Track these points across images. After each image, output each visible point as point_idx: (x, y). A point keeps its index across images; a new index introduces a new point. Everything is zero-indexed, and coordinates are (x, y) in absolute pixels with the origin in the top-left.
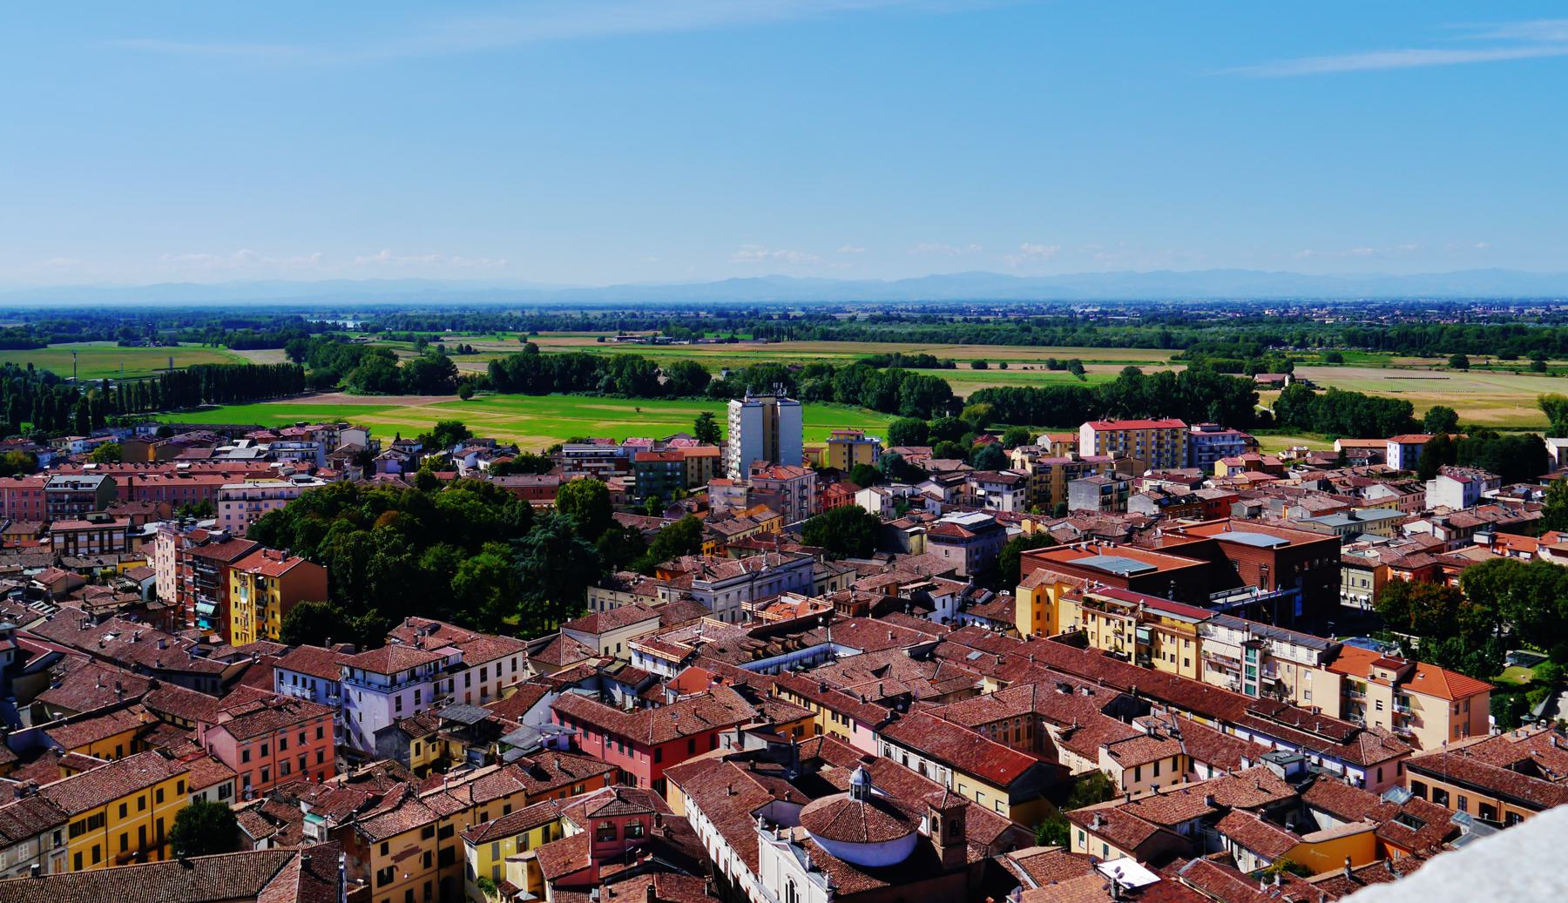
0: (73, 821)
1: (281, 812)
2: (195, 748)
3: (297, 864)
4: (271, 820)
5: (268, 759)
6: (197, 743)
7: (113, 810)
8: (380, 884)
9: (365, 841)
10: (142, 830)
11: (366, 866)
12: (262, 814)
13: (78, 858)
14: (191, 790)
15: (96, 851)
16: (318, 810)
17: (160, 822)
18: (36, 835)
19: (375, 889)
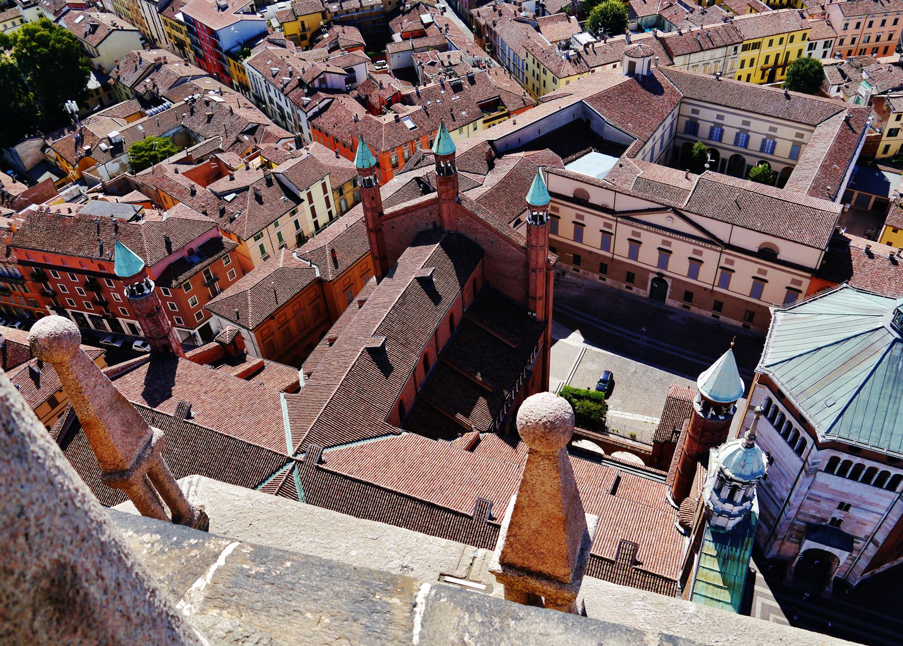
0: (745, 43)
1: (851, 73)
2: (821, 11)
3: (843, 115)
4: (844, 76)
5: (859, 31)
6: (823, 7)
7: (766, 42)
8: (888, 136)
9: (889, 110)
10: (778, 55)
11: (884, 123)
12: (840, 70)
13: (743, 62)
14: (809, 40)
15: (752, 60)
16: (871, 81)
17: (788, 53)
18: (726, 46)
19: (884, 137)
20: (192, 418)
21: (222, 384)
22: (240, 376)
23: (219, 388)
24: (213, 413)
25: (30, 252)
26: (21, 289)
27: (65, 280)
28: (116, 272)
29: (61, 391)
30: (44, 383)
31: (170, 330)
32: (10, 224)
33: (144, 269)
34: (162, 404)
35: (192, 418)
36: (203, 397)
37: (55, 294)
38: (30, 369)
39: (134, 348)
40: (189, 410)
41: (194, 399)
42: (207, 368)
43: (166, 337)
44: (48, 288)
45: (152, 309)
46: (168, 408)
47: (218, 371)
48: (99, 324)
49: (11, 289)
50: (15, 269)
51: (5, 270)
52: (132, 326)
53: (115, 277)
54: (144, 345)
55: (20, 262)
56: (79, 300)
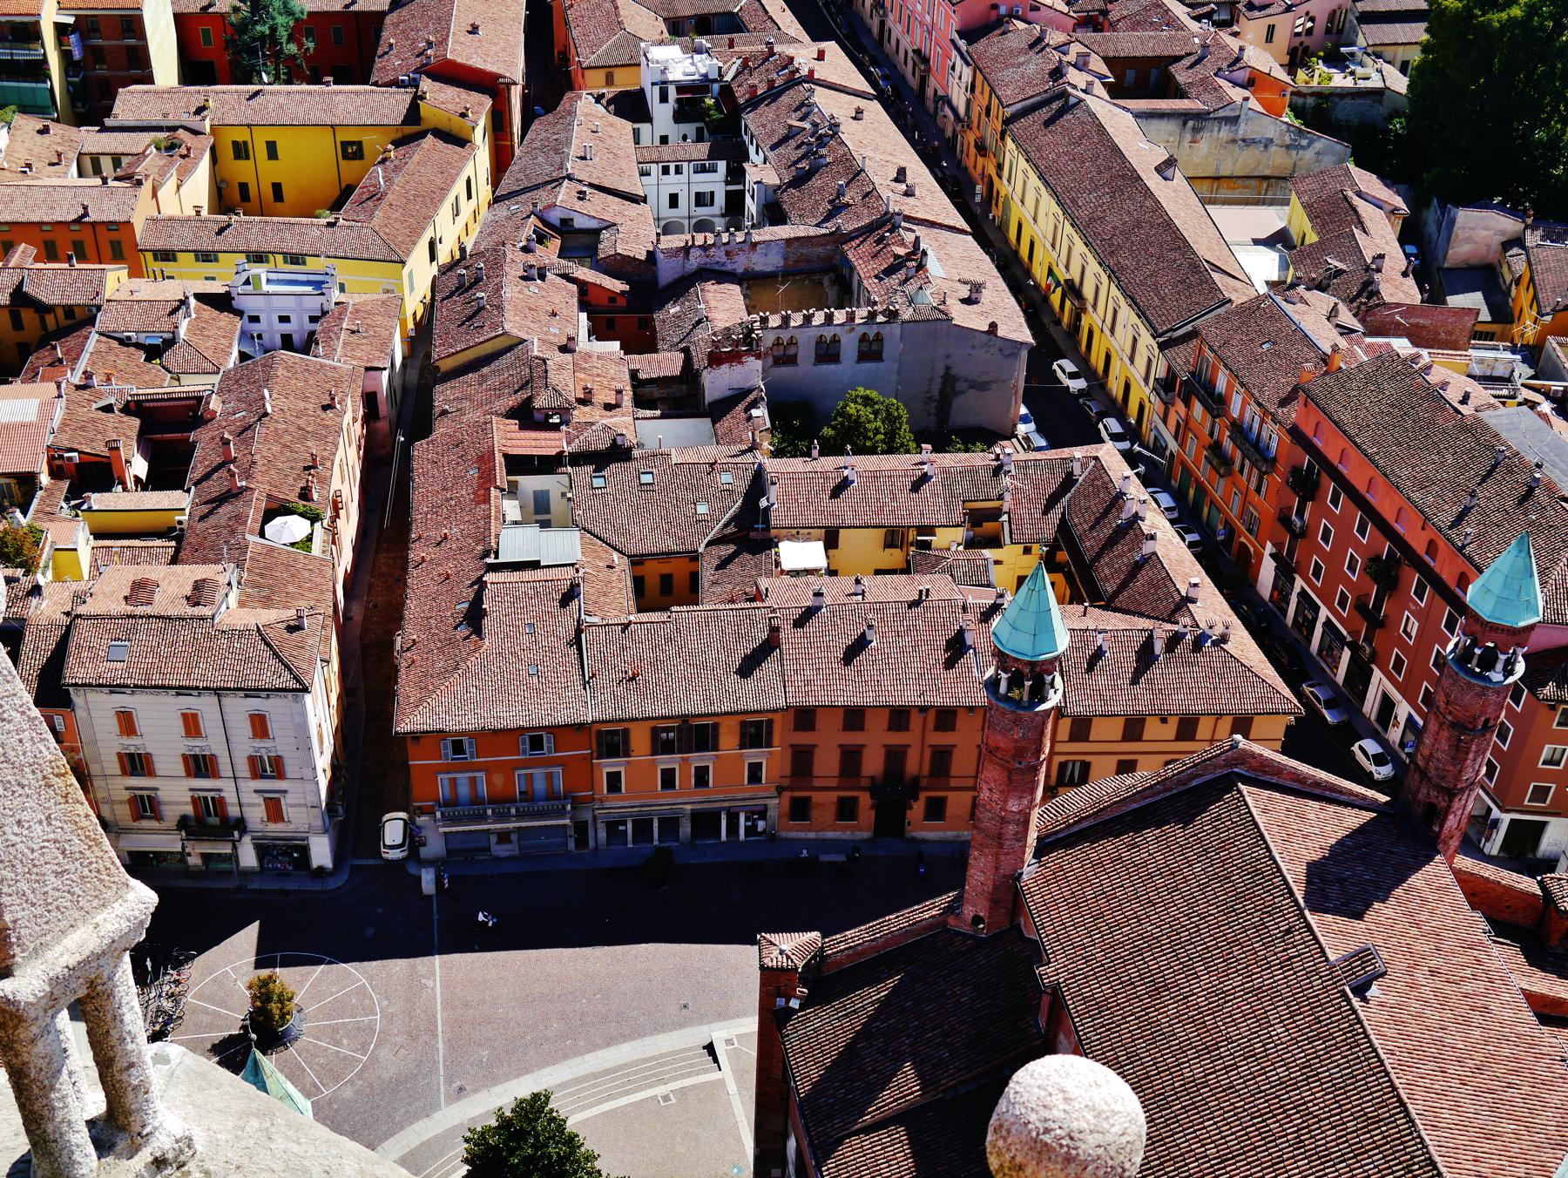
20: (1365, 1000)
21: (1481, 986)
22: (1533, 999)
23: (1468, 988)
24: (1413, 1028)
25: (1327, 424)
26: (1254, 480)
27: (1342, 523)
28: (1472, 595)
29: (1164, 721)
30: (1150, 682)
31: (1471, 785)
32: (1335, 348)
33: (1532, 627)
34: (1329, 917)
35: (1365, 1000)
36: (1421, 976)
37: (1303, 534)
38: (1150, 637)
39: (1355, 748)
40: (1376, 979)
41: (1398, 967)
42: (1479, 922)
43: (1451, 794)
44: (1300, 514)
45: (1475, 719)
46: (1336, 936)
47: (1496, 950)
48: (1330, 648)
49: (1237, 466)
50: (1273, 437)
51: (1256, 425)
52: (1387, 705)
53: (1461, 607)
54: (1379, 760)
55: (1295, 432)
56: (1336, 576)
